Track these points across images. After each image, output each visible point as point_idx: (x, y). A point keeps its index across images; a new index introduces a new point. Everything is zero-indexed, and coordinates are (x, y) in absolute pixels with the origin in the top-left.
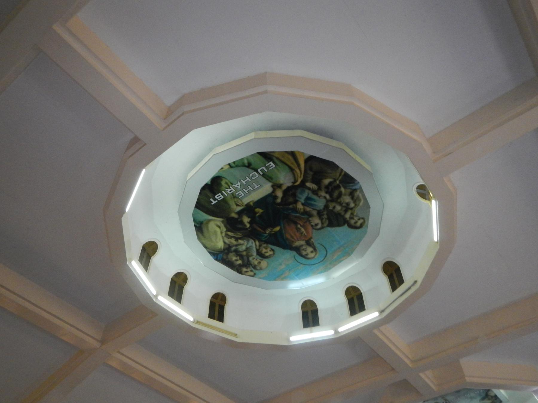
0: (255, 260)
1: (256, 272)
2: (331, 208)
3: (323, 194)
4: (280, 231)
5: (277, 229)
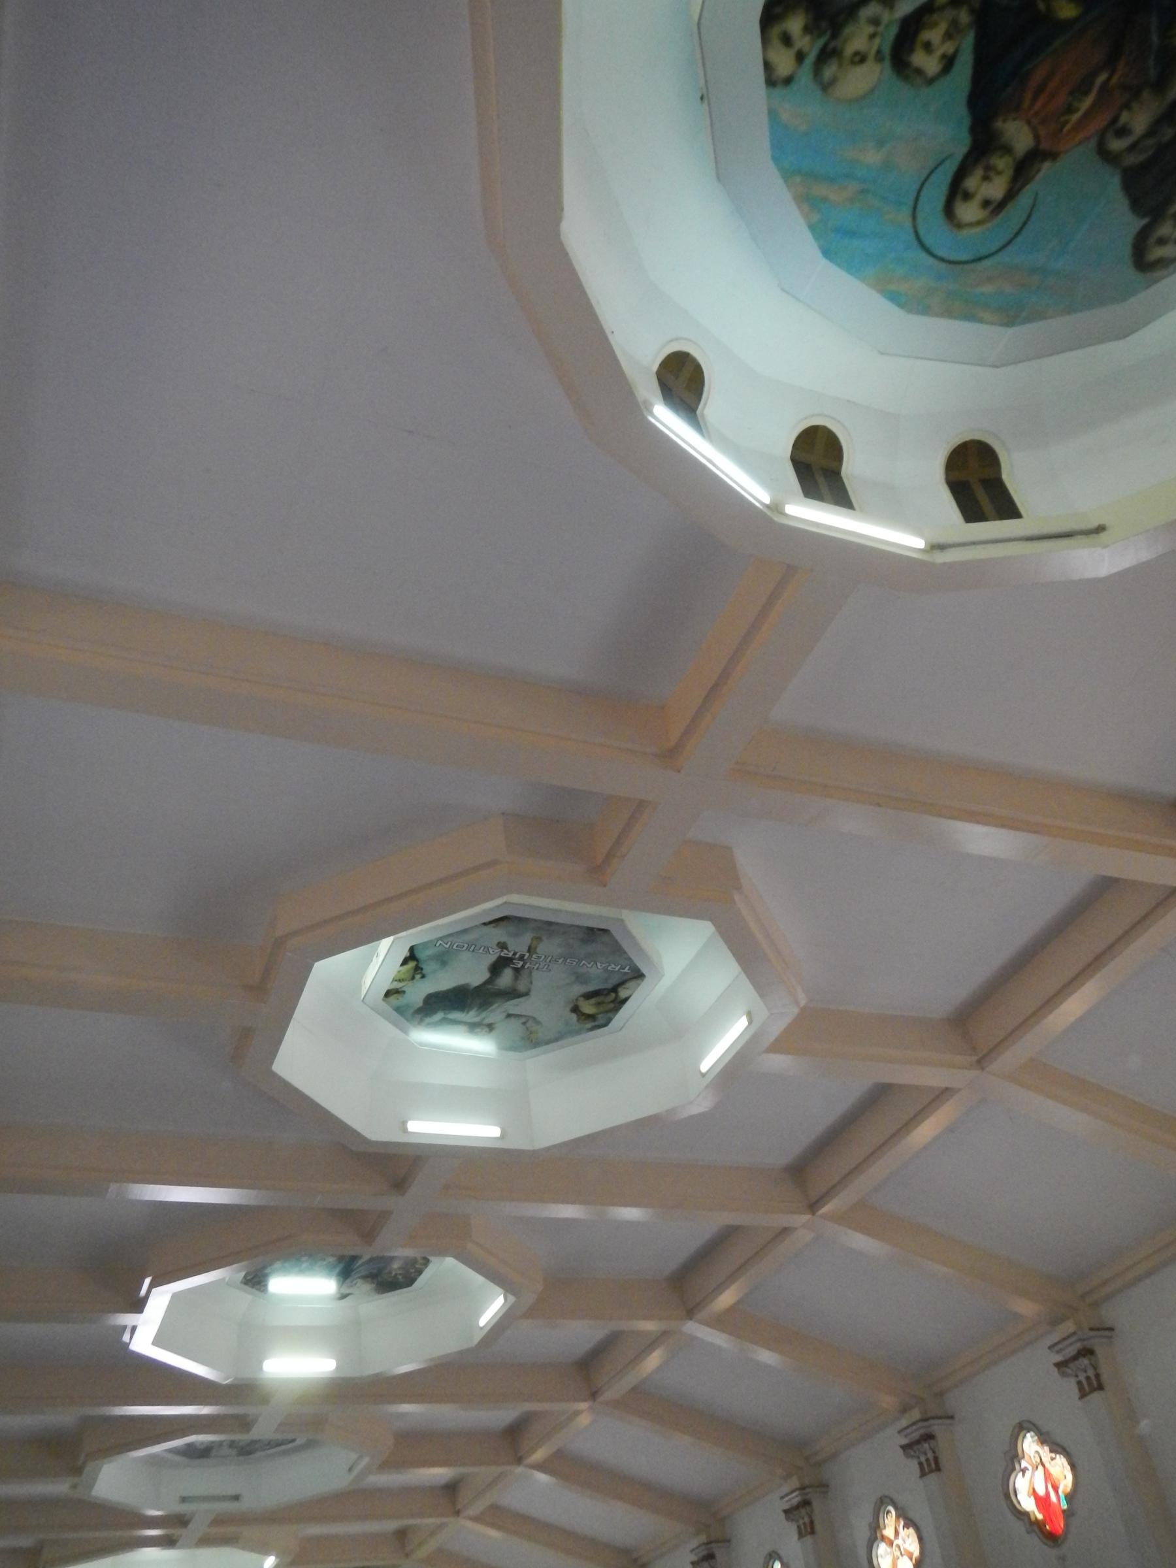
0: (871, 29)
1: (805, 75)
4: (1068, 24)
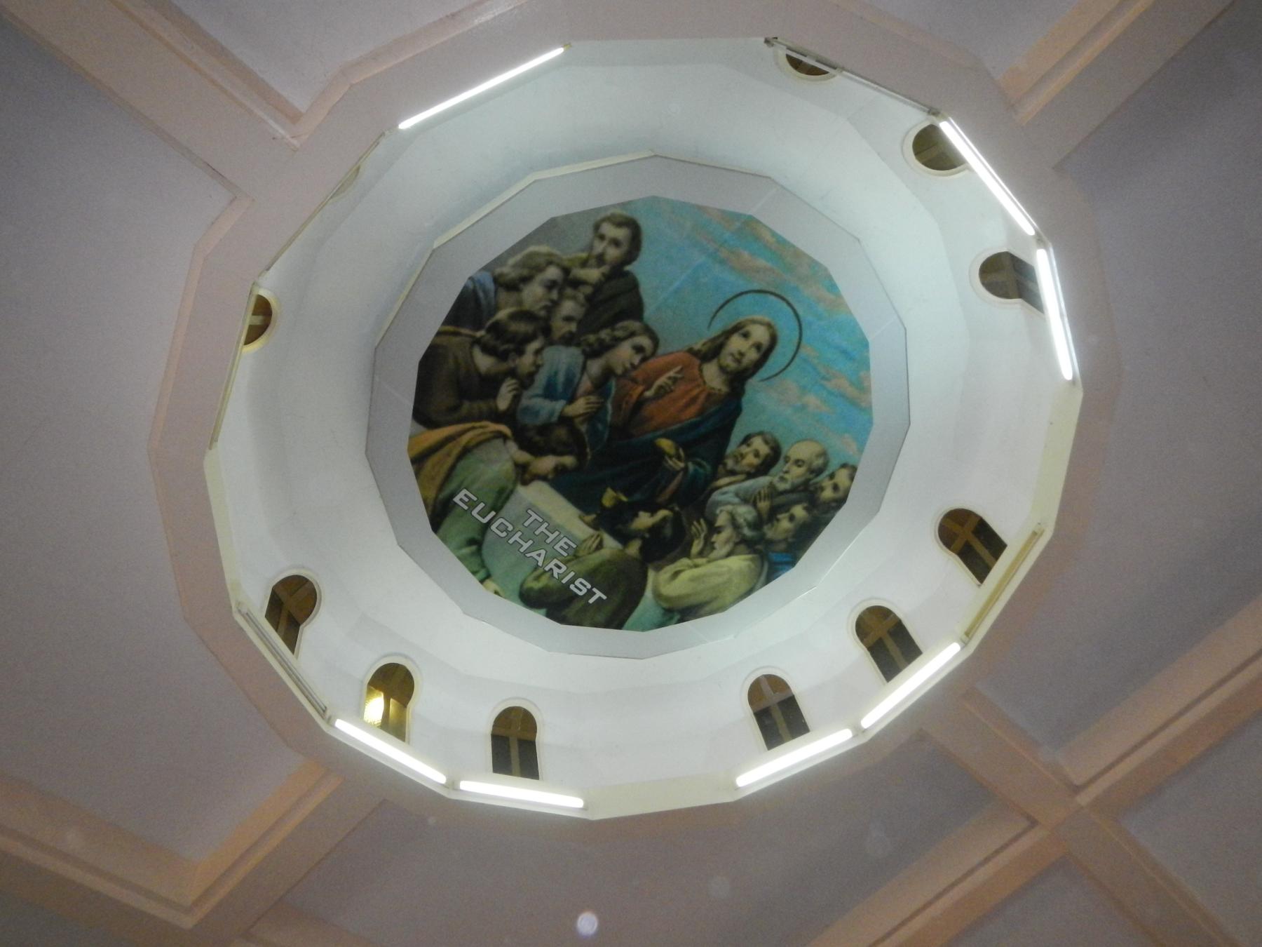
0: (787, 476)
1: (834, 464)
2: (573, 327)
3: (526, 362)
4: (667, 436)
5: (666, 444)
